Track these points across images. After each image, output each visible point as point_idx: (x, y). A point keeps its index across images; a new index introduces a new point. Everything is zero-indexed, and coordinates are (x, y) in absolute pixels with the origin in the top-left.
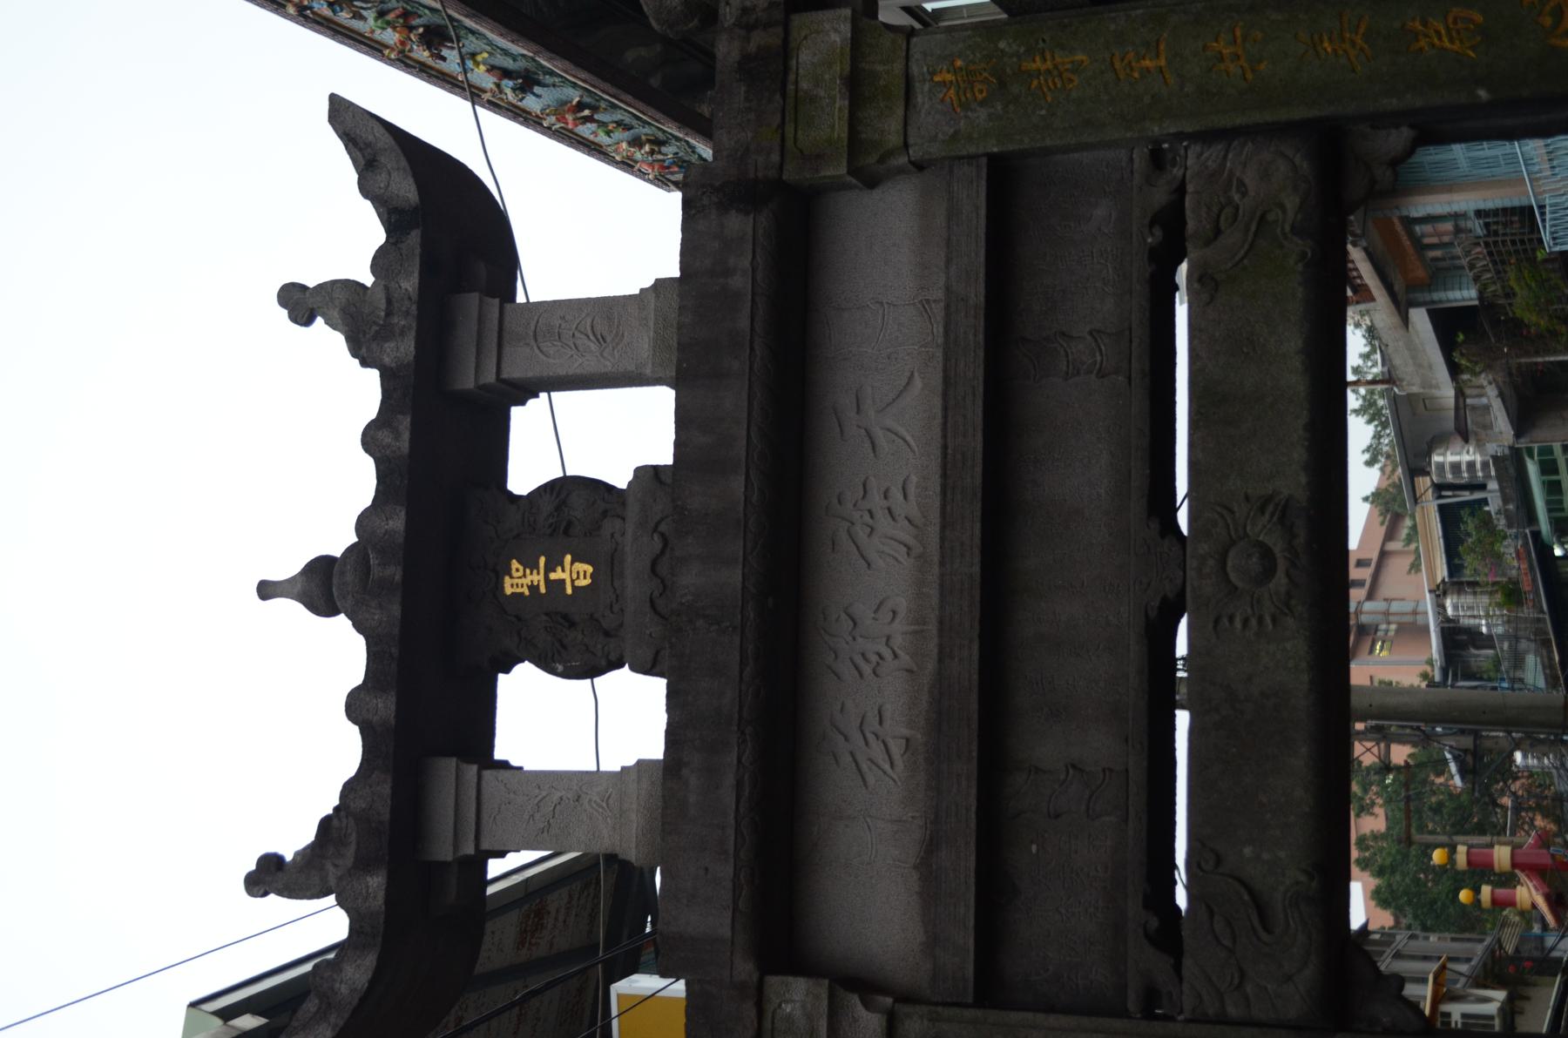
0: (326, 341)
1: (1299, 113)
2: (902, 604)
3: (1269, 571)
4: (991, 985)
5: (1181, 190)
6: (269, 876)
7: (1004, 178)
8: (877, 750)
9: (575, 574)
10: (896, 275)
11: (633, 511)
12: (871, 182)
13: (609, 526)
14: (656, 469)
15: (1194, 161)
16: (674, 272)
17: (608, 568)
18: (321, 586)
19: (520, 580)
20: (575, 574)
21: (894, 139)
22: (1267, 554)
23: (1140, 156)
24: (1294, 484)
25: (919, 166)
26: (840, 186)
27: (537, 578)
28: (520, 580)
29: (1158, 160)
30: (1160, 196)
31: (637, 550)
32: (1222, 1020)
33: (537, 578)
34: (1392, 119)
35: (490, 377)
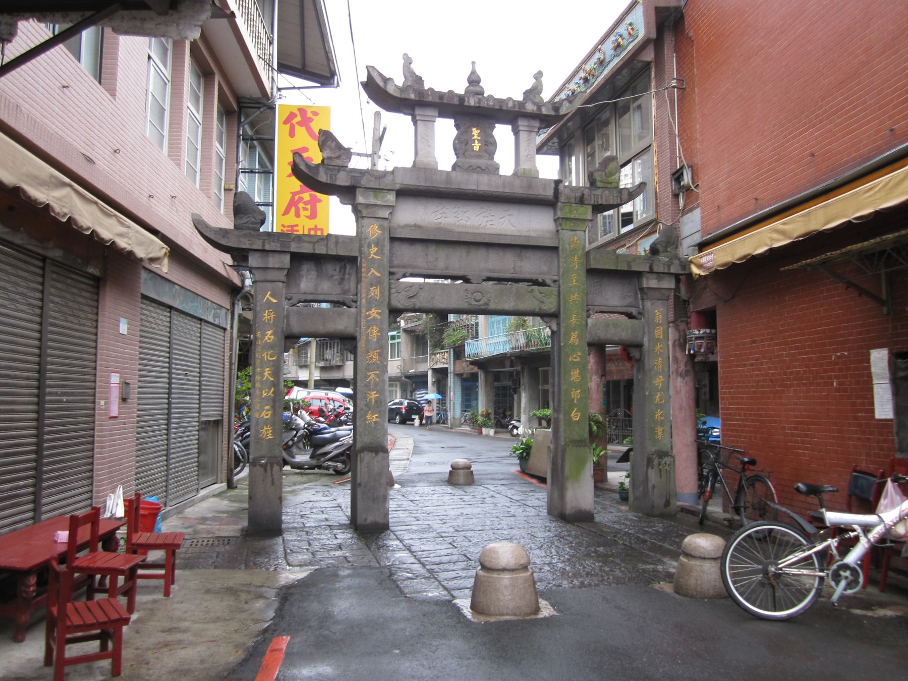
0: (529, 83)
1: (562, 310)
2: (469, 223)
3: (476, 301)
4: (393, 239)
5: (549, 286)
6: (408, 61)
7: (555, 249)
8: (439, 216)
9: (476, 146)
10: (534, 224)
11: (490, 162)
12: (555, 220)
13: (487, 155)
14: (498, 169)
15: (554, 289)
16: (540, 177)
17: (478, 155)
18: (474, 80)
19: (475, 132)
20: (476, 146)
21: (564, 227)
22: (479, 301)
23: (556, 278)
24: (492, 306)
25: (557, 231)
26: (555, 214)
27: (476, 137)
28: (475, 132)
29: (555, 281)
30: (548, 282)
31: (482, 162)
32: (390, 289)
33: (476, 137)
34: (559, 328)
35: (521, 128)
